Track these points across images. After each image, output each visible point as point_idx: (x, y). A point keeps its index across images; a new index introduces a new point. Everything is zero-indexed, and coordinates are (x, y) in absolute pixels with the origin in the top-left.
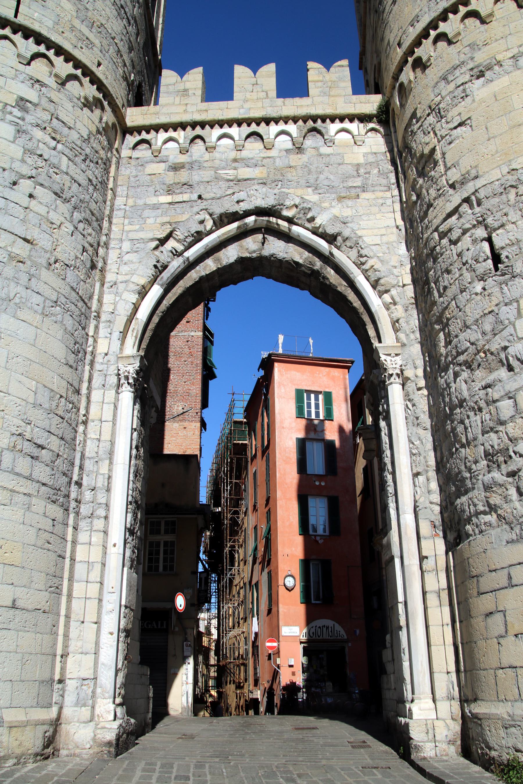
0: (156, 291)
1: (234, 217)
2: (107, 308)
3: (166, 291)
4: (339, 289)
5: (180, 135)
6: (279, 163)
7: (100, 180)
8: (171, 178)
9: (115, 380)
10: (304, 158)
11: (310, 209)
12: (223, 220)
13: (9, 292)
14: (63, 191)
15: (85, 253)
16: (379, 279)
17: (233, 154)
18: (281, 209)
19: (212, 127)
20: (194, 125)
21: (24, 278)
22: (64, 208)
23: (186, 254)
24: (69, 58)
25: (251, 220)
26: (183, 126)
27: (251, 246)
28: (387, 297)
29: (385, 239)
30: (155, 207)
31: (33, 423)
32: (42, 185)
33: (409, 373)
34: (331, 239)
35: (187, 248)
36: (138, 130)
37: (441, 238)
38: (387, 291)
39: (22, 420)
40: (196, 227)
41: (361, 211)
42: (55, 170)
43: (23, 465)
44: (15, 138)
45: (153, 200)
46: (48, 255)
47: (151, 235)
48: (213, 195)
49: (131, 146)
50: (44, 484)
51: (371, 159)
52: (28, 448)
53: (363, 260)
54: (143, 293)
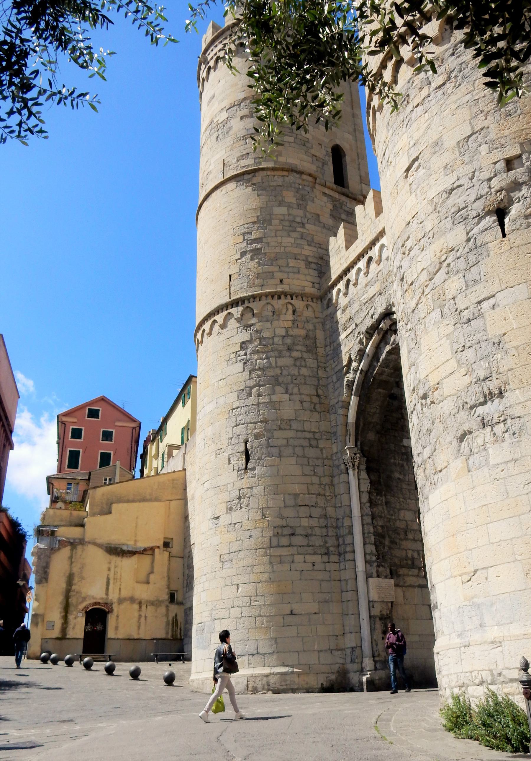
0: (354, 400)
6: (385, 272)
7: (304, 349)
9: (343, 467)
12: (369, 333)
14: (277, 380)
15: (304, 404)
18: (391, 308)
19: (353, 267)
22: (278, 389)
23: (360, 368)
35: (359, 364)
40: (357, 347)
42: (269, 370)
43: (284, 541)
44: (244, 368)
48: (361, 319)
49: (325, 307)
54: (347, 405)
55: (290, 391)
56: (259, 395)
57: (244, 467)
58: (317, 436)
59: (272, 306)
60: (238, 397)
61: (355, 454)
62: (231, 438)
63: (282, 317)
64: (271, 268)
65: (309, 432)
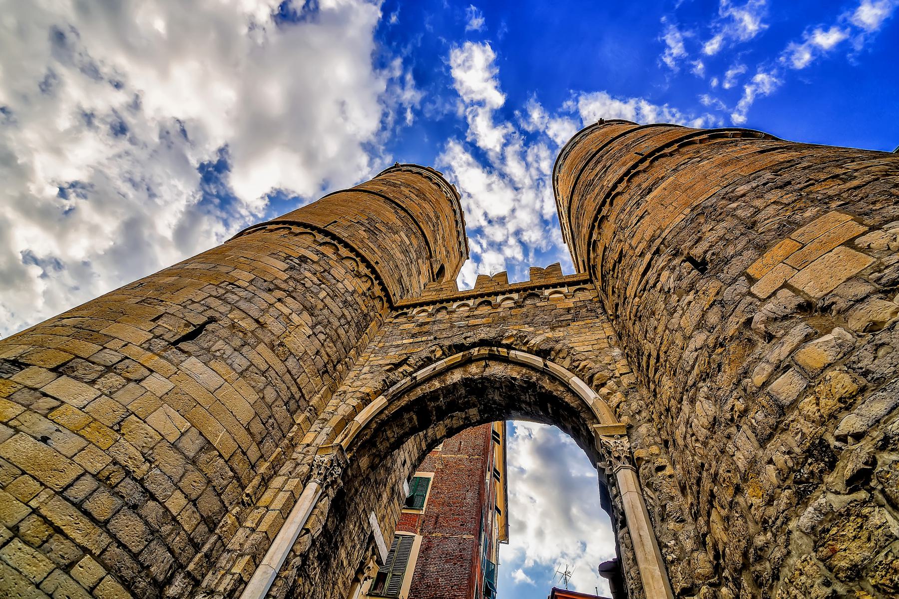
0: (380, 402)
1: (460, 348)
2: (330, 409)
3: (390, 402)
4: (555, 393)
5: (430, 309)
8: (417, 330)
10: (525, 310)
11: (526, 336)
13: (213, 345)
16: (593, 375)
17: (467, 314)
20: (441, 301)
21: (237, 342)
23: (414, 375)
24: (352, 250)
25: (475, 351)
26: (433, 303)
27: (474, 370)
28: (604, 391)
29: (596, 347)
30: (398, 346)
31: (157, 463)
32: (294, 298)
33: (640, 453)
34: (544, 353)
35: (416, 371)
36: (402, 308)
37: (640, 297)
38: (603, 385)
39: (143, 454)
40: (424, 354)
41: (572, 332)
44: (286, 270)
45: (399, 342)
46: (274, 338)
47: (388, 362)
50: (120, 545)
51: (579, 304)
52: (128, 487)
53: (576, 364)
54: (366, 400)
55: (315, 330)
56: (279, 300)
57: (172, 340)
58: (302, 403)
59: (358, 265)
60: (252, 280)
61: (339, 465)
62: (193, 302)
63: (359, 281)
64: (376, 249)
65: (300, 389)
